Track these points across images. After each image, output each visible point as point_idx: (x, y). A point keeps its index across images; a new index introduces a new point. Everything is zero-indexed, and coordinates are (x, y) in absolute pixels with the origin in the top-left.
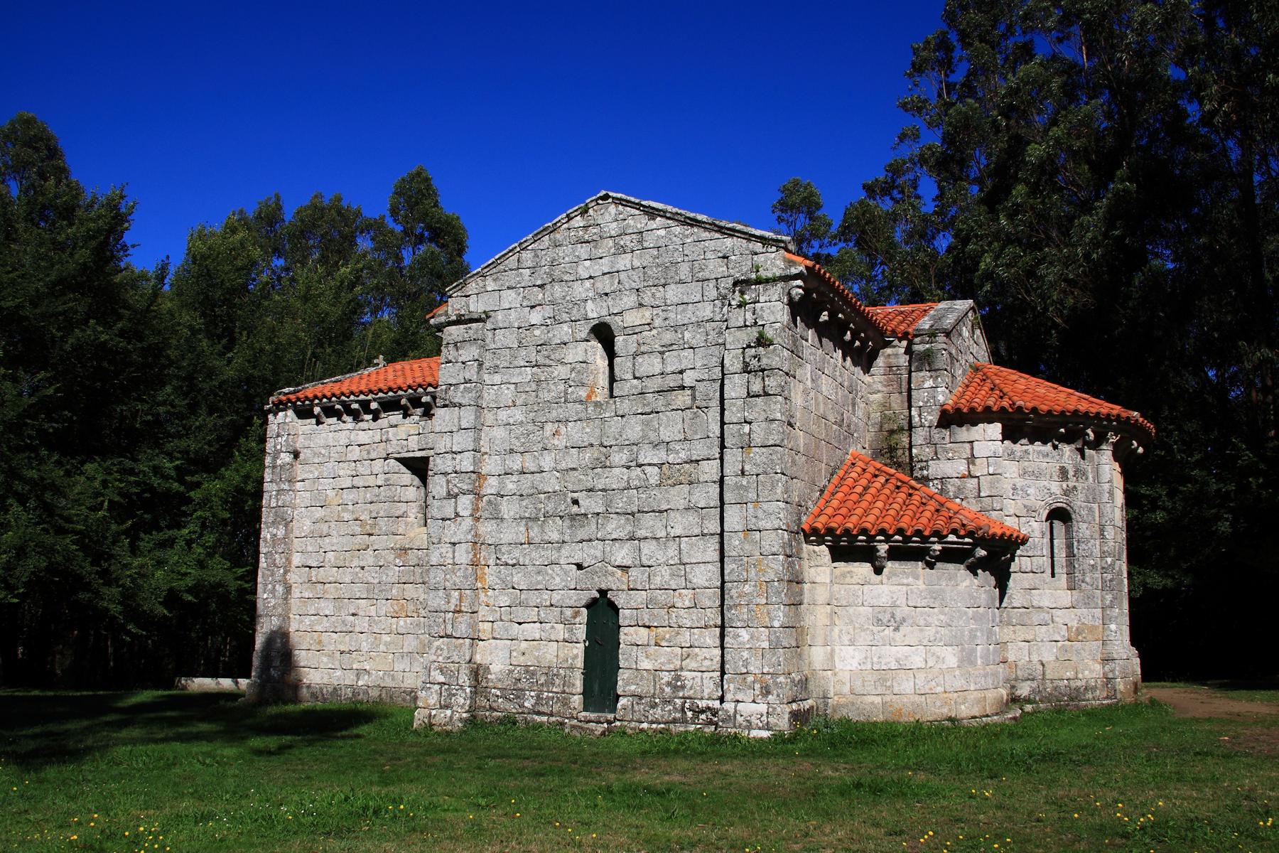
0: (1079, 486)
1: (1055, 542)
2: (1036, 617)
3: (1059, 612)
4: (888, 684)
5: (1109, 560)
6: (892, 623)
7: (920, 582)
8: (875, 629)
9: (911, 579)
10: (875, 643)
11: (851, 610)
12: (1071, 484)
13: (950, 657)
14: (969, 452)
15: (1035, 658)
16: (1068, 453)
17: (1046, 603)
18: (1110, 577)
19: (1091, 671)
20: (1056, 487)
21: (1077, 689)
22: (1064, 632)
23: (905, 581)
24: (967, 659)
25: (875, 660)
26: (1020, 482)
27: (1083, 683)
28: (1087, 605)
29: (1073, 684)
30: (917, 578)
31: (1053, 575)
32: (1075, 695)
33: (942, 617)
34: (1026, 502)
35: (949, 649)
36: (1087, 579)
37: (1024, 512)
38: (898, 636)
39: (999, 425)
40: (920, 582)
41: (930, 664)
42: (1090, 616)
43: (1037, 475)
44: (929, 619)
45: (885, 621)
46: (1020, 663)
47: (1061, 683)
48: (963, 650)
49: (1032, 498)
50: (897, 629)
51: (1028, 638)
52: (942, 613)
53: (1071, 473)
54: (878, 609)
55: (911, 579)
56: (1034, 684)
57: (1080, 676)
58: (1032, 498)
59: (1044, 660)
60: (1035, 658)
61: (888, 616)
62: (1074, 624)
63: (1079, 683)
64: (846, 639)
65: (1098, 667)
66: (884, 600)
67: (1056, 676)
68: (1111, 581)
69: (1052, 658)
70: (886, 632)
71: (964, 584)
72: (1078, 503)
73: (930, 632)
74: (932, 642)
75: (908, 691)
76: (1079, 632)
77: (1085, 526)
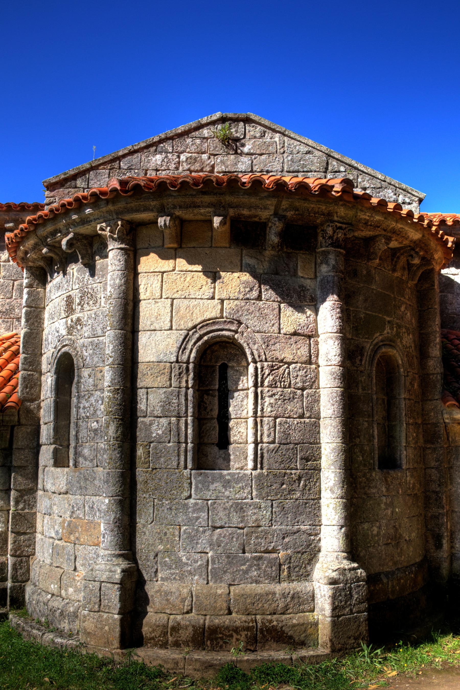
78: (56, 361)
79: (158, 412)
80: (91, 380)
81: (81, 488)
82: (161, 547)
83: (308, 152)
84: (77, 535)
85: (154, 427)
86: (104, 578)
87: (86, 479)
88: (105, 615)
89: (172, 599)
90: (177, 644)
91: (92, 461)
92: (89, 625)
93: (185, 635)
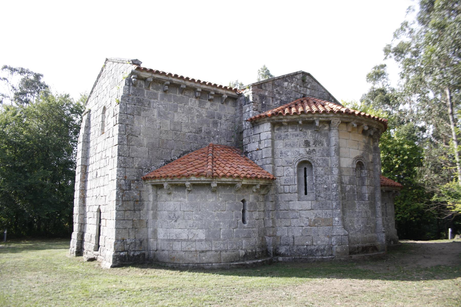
0: (317, 149)
1: (307, 177)
2: (291, 215)
3: (304, 212)
4: (171, 246)
5: (335, 185)
6: (174, 218)
7: (186, 200)
8: (168, 221)
9: (182, 198)
10: (168, 227)
11: (161, 212)
12: (311, 149)
13: (202, 235)
14: (259, 138)
15: (291, 235)
16: (310, 133)
17: (297, 207)
18: (334, 193)
19: (322, 241)
20: (302, 151)
21: (311, 250)
22: (306, 221)
23: (180, 199)
24: (212, 236)
25: (168, 234)
26: (284, 150)
27: (316, 247)
28: (321, 208)
29: (309, 248)
30: (185, 198)
31: (306, 193)
32: (311, 253)
33: (197, 216)
34: (287, 159)
35: (201, 230)
36: (322, 195)
37: (285, 164)
38: (176, 224)
39: (269, 124)
40: (186, 200)
41: (190, 237)
42: (322, 214)
43: (292, 146)
44: (191, 217)
45: (172, 217)
46: (283, 237)
47: (302, 247)
48: (209, 231)
49: (290, 157)
50: (176, 221)
51: (287, 225)
52: (197, 214)
53: (312, 143)
54: (169, 212)
55: (182, 198)
56: (288, 248)
57: (315, 243)
58: (290, 157)
59: (295, 235)
60: (291, 235)
61: (173, 215)
62: (313, 218)
63: (313, 247)
64: (160, 225)
65: (327, 239)
66: (172, 208)
67: (300, 243)
68: (336, 195)
69: (299, 235)
70: (172, 222)
71: (211, 200)
72: (317, 157)
73: (191, 222)
74: (192, 227)
75: (178, 249)
76: (315, 221)
77: (320, 169)
78: (297, 163)
79: (348, 183)
80: (323, 171)
81: (320, 207)
82: (350, 224)
83: (324, 92)
84: (319, 223)
85: (347, 188)
86: (343, 234)
87: (322, 204)
88: (344, 246)
89: (355, 239)
90: (358, 253)
91: (325, 198)
92: (338, 250)
93: (360, 249)
